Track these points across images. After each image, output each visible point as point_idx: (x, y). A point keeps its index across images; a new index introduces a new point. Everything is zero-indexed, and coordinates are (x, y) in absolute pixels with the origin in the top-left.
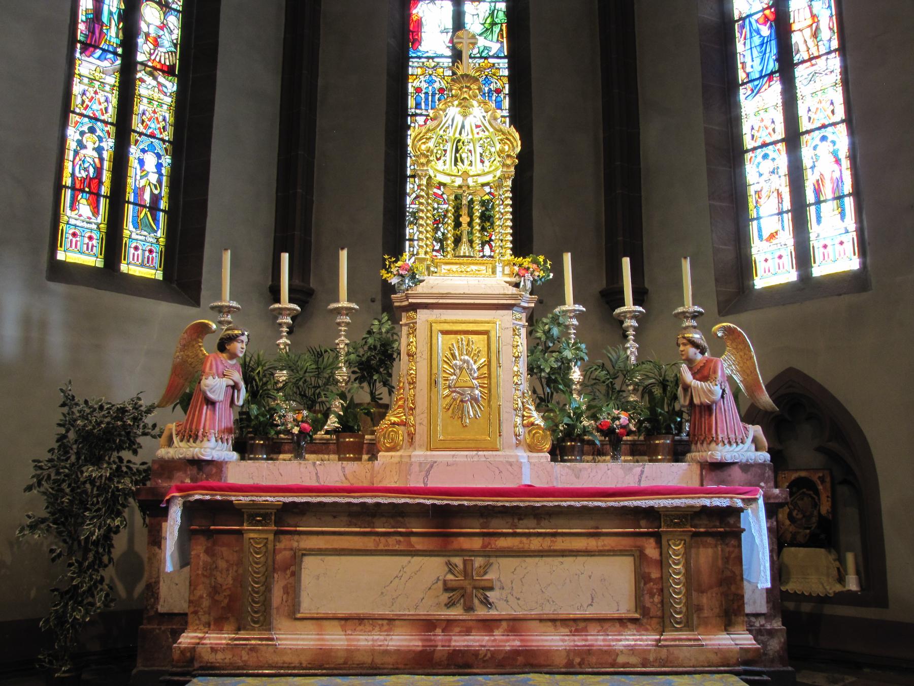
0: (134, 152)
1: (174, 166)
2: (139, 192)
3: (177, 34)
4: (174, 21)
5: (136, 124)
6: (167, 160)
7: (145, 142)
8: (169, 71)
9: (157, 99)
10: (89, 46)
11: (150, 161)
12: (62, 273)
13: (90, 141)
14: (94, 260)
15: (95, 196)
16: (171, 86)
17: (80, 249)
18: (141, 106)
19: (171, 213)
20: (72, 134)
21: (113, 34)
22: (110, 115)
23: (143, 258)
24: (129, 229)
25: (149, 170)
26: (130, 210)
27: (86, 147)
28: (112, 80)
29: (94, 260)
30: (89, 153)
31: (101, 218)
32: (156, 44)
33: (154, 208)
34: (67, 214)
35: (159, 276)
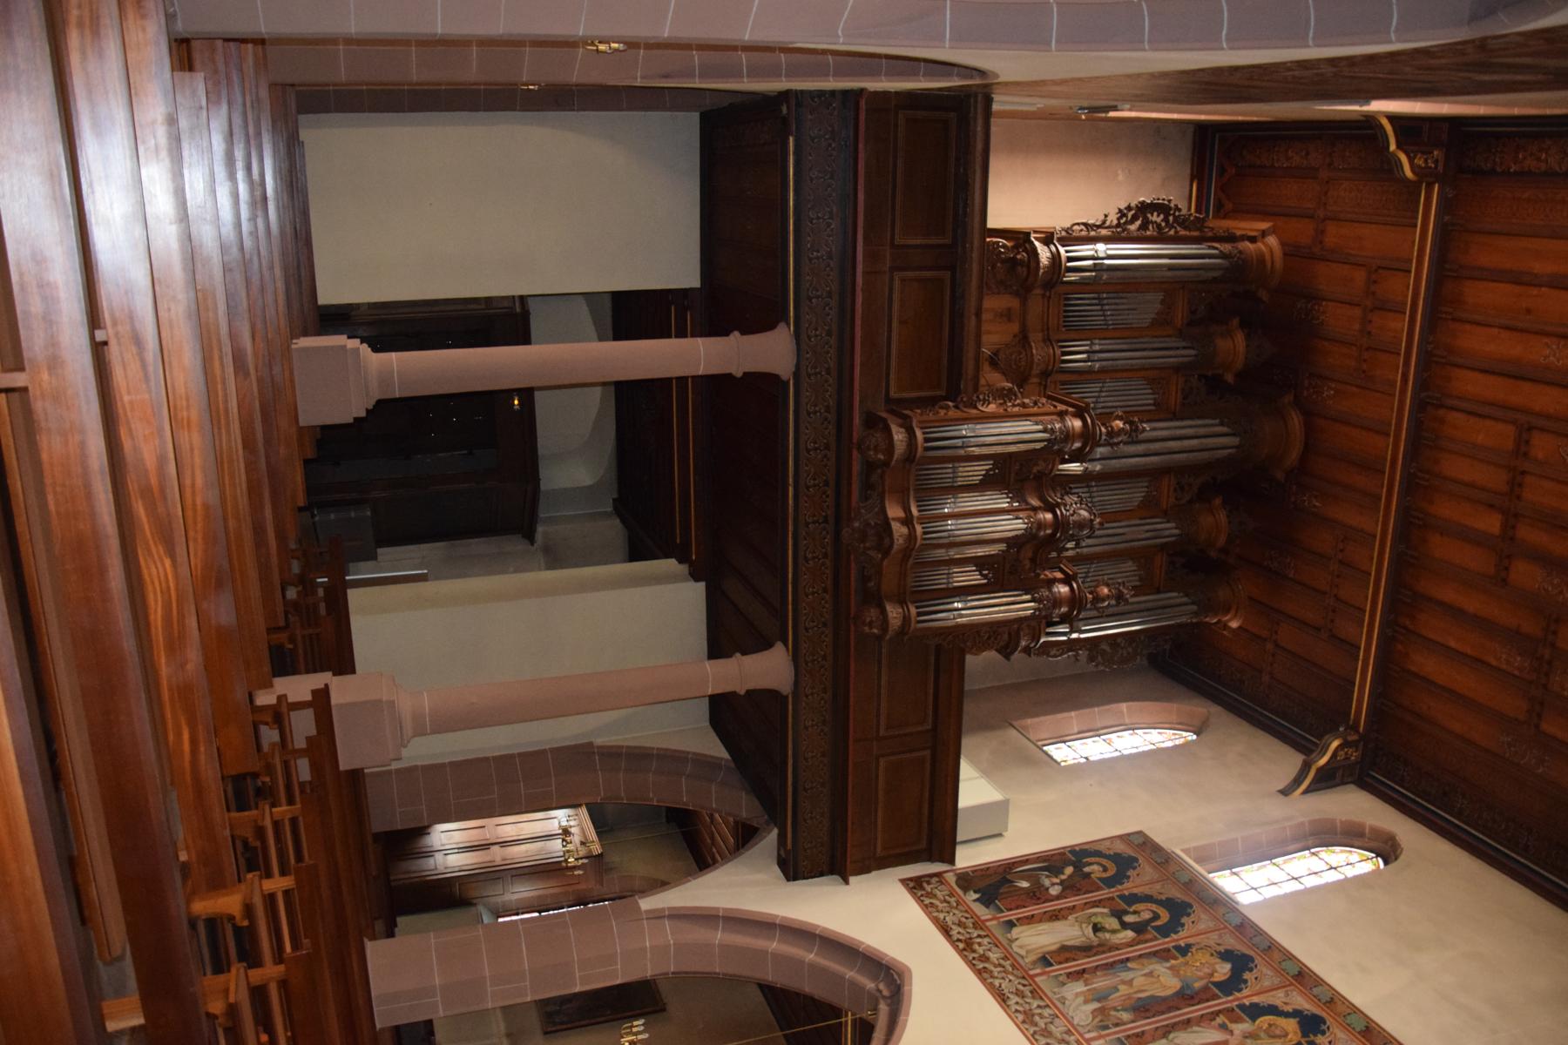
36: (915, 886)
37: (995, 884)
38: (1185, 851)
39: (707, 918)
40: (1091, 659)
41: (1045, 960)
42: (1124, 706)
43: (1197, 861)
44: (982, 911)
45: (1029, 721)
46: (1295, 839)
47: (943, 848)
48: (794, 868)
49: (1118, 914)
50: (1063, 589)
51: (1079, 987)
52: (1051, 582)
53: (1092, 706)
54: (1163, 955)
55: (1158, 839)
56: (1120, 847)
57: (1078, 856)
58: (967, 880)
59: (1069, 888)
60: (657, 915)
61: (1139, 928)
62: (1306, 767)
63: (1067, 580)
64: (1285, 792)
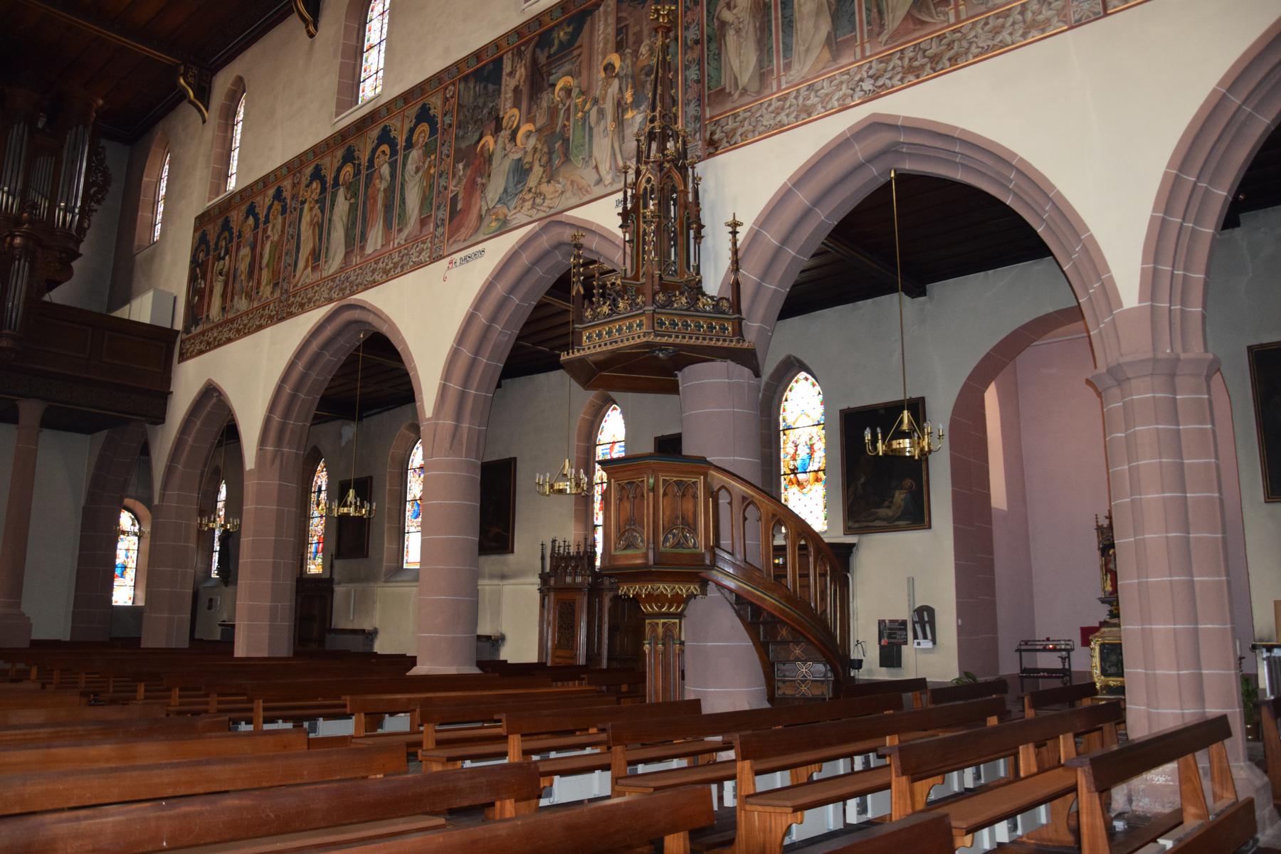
36: (183, 358)
37: (194, 313)
38: (210, 200)
39: (170, 470)
40: (98, 202)
41: (223, 309)
42: (145, 179)
43: (218, 195)
44: (200, 329)
45: (136, 243)
46: (226, 131)
47: (172, 333)
48: (159, 417)
49: (220, 258)
50: (18, 241)
51: (236, 298)
52: (11, 244)
53: (138, 200)
54: (238, 249)
55: (200, 212)
56: (198, 235)
57: (194, 262)
58: (187, 329)
59: (204, 277)
60: (163, 496)
61: (227, 252)
62: (191, 102)
63: (14, 237)
64: (204, 122)
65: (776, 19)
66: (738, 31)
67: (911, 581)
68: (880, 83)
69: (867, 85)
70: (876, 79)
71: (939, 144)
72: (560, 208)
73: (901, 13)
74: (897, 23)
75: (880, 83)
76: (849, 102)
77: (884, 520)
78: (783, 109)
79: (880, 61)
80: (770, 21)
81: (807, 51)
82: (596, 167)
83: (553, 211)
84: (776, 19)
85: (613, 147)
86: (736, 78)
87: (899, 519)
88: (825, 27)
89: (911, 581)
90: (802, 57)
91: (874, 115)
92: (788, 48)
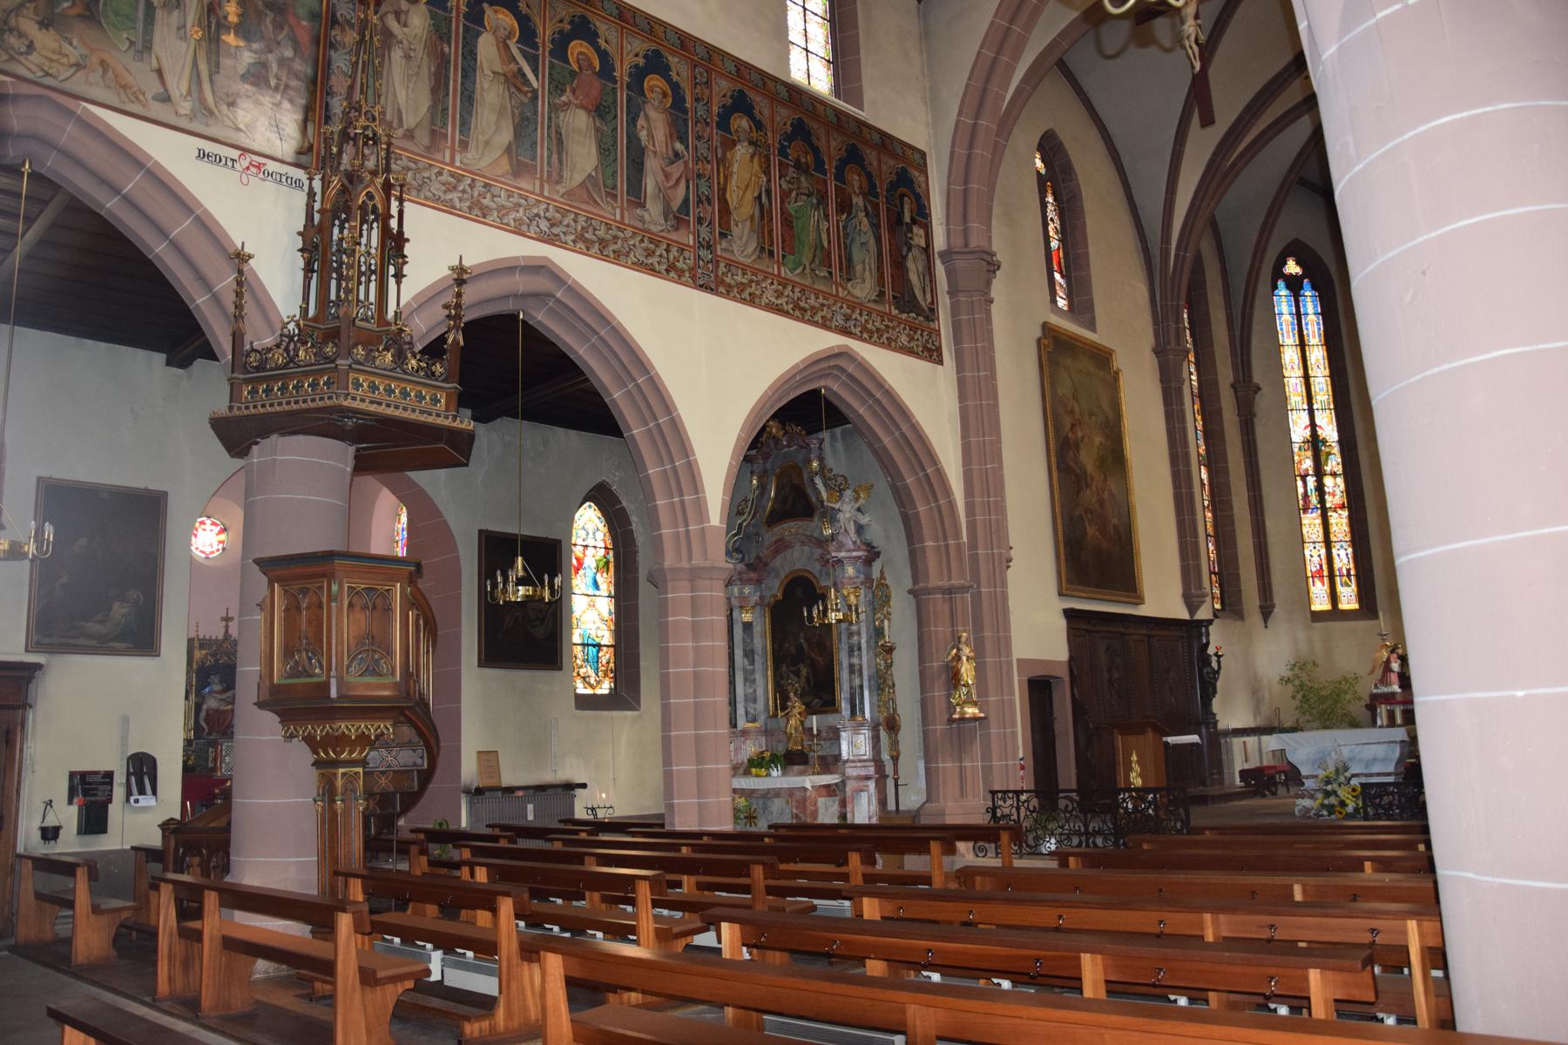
0: (1334, 551)
1: (1354, 553)
2: (1340, 570)
3: (1342, 486)
4: (1340, 481)
5: (1333, 538)
6: (1350, 550)
7: (1338, 545)
8: (1342, 507)
9: (1340, 523)
10: (1305, 510)
11: (1342, 553)
12: (1318, 616)
13: (1315, 553)
14: (1327, 606)
15: (1322, 577)
16: (1345, 513)
17: (1321, 603)
18: (1333, 528)
19: (1357, 575)
20: (1307, 552)
21: (1314, 500)
22: (1321, 538)
23: (1349, 599)
24: (1339, 588)
25: (1343, 558)
26: (1338, 579)
27: (1314, 556)
28: (1319, 521)
29: (1327, 606)
30: (1316, 559)
31: (1327, 587)
32: (1333, 495)
33: (1349, 575)
34: (1313, 589)
35: (1356, 606)
65: (455, 81)
66: (408, 57)
67: (126, 720)
68: (555, 230)
69: (544, 225)
70: (552, 225)
71: (588, 319)
72: (69, 86)
73: (579, 178)
74: (575, 184)
75: (555, 230)
76: (524, 228)
77: (93, 638)
78: (455, 188)
79: (557, 210)
80: (447, 77)
81: (487, 143)
82: (159, 72)
83: (48, 81)
84: (455, 81)
85: (195, 64)
86: (400, 111)
87: (114, 640)
88: (506, 136)
89: (126, 720)
90: (481, 146)
91: (546, 258)
92: (465, 125)
